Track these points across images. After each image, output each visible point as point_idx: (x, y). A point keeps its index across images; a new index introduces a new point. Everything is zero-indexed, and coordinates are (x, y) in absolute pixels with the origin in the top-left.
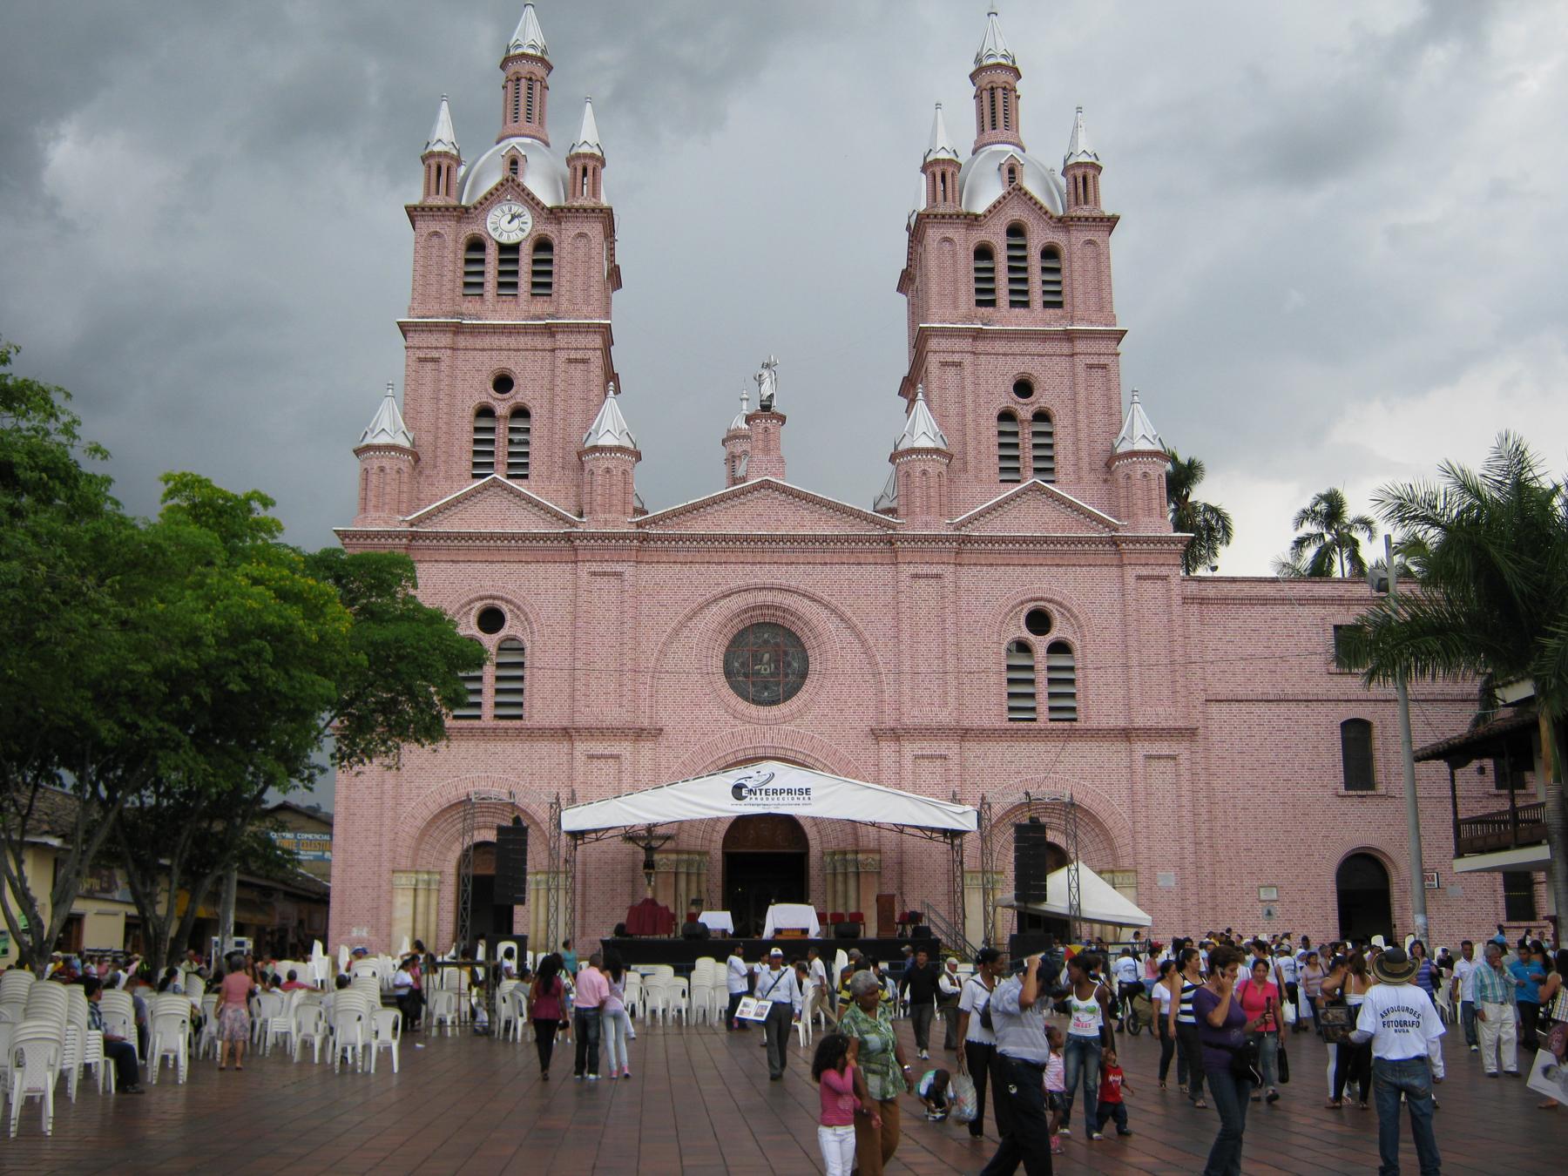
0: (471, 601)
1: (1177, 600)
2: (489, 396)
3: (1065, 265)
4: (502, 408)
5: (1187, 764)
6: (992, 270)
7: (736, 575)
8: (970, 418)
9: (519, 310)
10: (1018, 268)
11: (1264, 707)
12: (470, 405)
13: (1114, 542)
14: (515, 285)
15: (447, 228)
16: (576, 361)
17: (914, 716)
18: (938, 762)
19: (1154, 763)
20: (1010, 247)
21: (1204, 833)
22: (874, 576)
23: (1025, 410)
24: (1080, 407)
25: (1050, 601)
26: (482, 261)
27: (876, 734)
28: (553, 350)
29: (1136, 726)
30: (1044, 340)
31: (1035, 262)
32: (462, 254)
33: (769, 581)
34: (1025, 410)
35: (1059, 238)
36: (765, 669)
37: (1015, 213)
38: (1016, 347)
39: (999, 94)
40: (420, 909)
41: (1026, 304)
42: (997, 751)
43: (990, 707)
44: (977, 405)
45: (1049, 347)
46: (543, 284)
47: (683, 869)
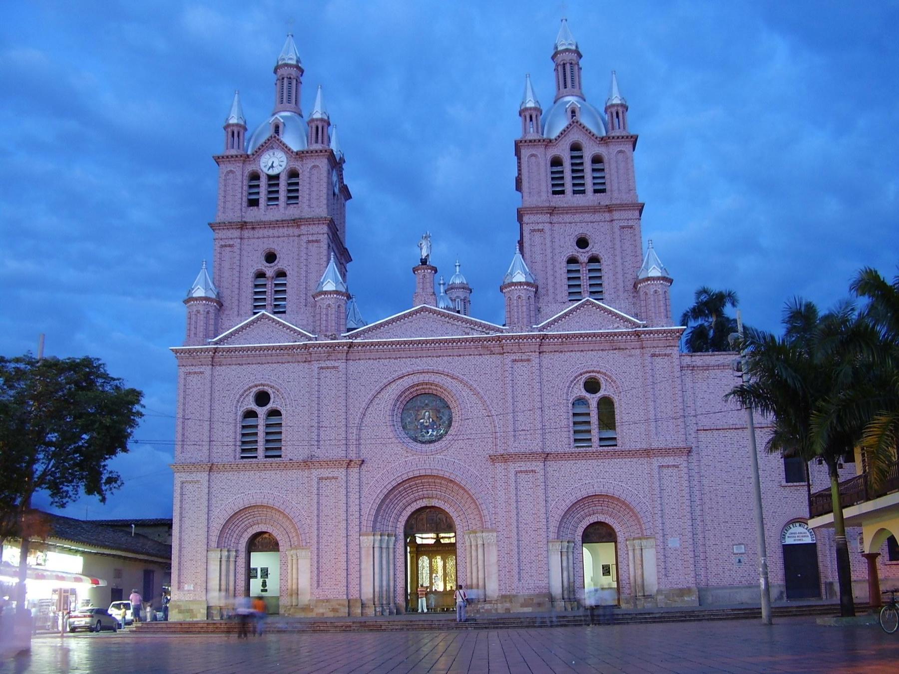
0: (251, 388)
1: (678, 368)
2: (263, 266)
3: (606, 166)
4: (270, 271)
5: (686, 470)
6: (562, 172)
7: (405, 365)
8: (549, 262)
9: (282, 211)
10: (577, 169)
11: (734, 432)
12: (252, 271)
13: (637, 334)
14: (277, 199)
15: (237, 167)
16: (313, 241)
17: (514, 447)
18: (531, 475)
19: (665, 470)
20: (572, 158)
21: (698, 512)
22: (490, 361)
23: (583, 256)
24: (618, 252)
25: (599, 372)
26: (258, 186)
27: (493, 459)
28: (299, 236)
29: (653, 447)
30: (575, 214)
31: (588, 166)
32: (246, 182)
33: (426, 368)
34: (583, 256)
35: (601, 150)
37: (575, 136)
38: (578, 217)
39: (568, 67)
40: (224, 573)
41: (583, 192)
42: (568, 466)
43: (562, 440)
44: (554, 255)
45: (597, 217)
46: (293, 197)
47: (377, 545)
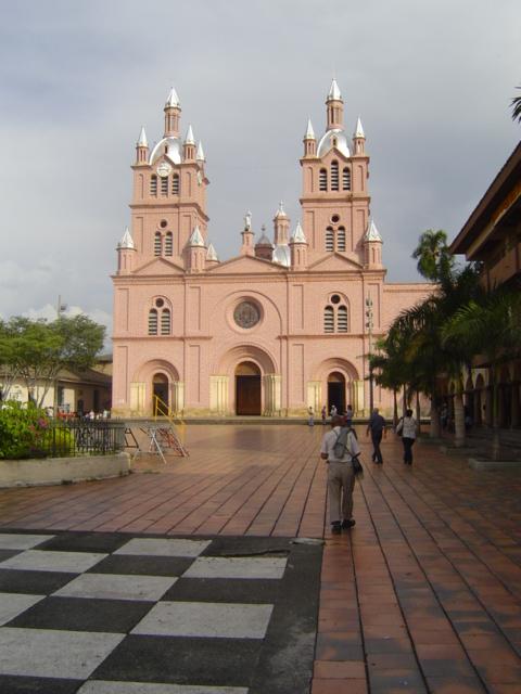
7: (236, 287)
27: (280, 338)
31: (341, 173)
34: (335, 226)
35: (349, 165)
36: (246, 317)
37: (334, 157)
38: (333, 204)
46: (177, 191)
